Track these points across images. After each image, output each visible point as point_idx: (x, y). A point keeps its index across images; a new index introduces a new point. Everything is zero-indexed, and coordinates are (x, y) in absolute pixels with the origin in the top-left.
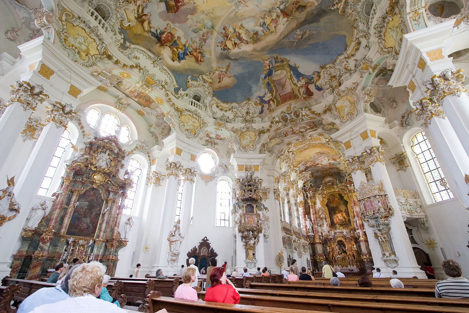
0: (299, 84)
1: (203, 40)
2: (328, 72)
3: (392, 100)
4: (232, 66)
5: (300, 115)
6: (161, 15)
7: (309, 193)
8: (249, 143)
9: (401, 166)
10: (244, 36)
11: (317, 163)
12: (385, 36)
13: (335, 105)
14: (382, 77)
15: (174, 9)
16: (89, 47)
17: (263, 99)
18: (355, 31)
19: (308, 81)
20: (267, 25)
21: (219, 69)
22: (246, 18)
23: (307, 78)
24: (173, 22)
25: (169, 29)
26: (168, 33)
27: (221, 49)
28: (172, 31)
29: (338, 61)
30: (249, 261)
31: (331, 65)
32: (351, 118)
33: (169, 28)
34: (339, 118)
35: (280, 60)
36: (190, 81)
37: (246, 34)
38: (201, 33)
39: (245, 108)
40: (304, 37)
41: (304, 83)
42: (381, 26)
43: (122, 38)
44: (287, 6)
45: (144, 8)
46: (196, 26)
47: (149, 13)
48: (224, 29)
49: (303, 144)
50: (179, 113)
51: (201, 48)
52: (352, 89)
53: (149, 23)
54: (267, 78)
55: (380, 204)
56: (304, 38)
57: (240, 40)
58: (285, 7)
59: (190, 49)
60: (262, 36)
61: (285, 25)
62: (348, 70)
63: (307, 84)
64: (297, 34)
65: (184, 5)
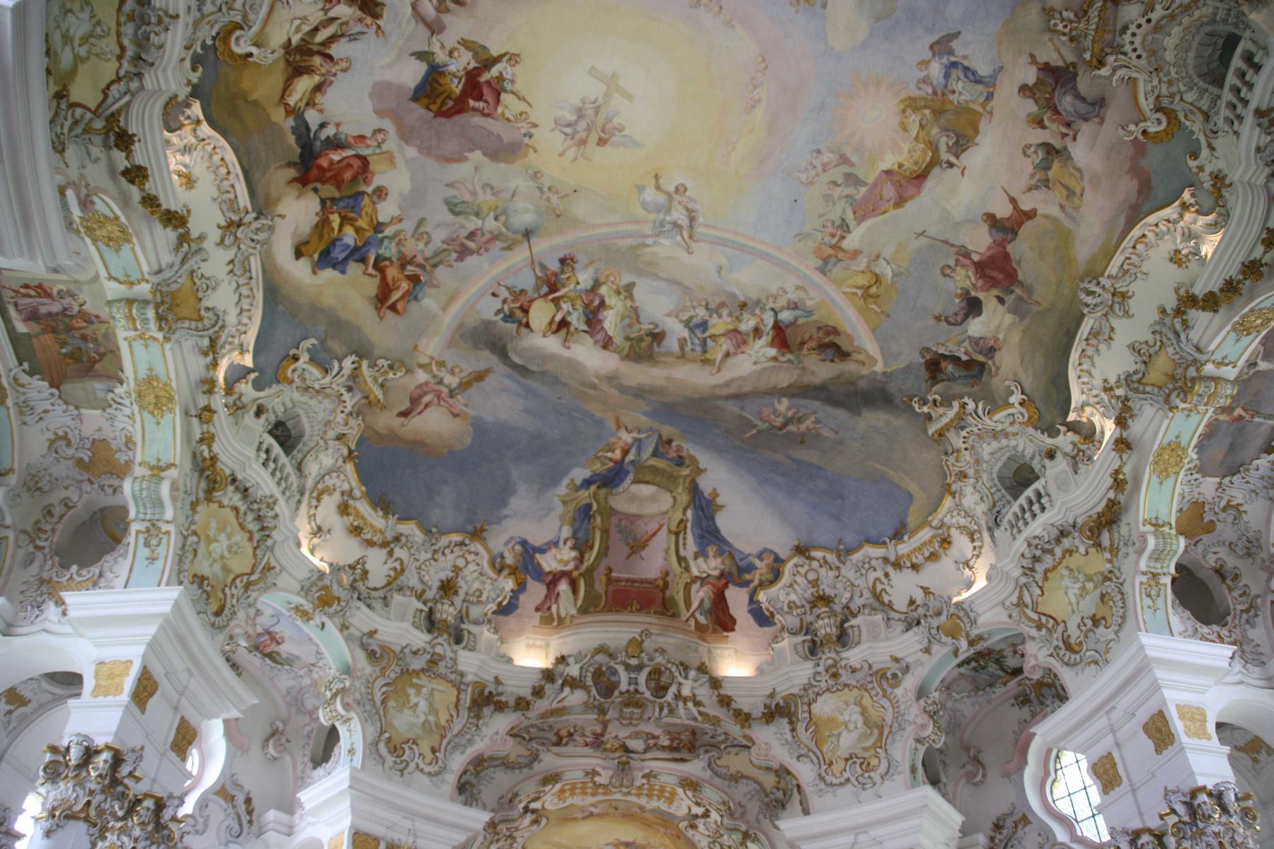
0: (698, 567)
1: (458, 248)
2: (811, 576)
3: (972, 752)
4: (490, 381)
5: (673, 690)
6: (381, 92)
8: (420, 731)
10: (610, 321)
12: (1046, 579)
13: (809, 705)
14: (973, 673)
15: (443, 104)
16: (82, 69)
17: (533, 558)
18: (948, 502)
19: (734, 570)
20: (707, 334)
21: (434, 369)
22: (660, 278)
23: (733, 558)
24: (406, 135)
25: (368, 146)
26: (357, 156)
27: (499, 311)
28: (375, 158)
29: (857, 557)
31: (831, 558)
32: (861, 779)
33: (375, 144)
34: (816, 761)
35: (672, 454)
36: (305, 357)
37: (623, 318)
38: (473, 223)
39: (449, 560)
40: (791, 428)
41: (716, 573)
42: (1047, 546)
43: (189, 83)
44: (800, 321)
45: (343, 35)
46: (474, 194)
47: (348, 60)
48: (563, 261)
49: (594, 795)
50: (203, 485)
51: (428, 268)
52: (884, 676)
53: (319, 88)
54: (593, 488)
56: (789, 433)
57: (589, 322)
58: (793, 324)
59: (389, 250)
60: (669, 354)
61: (758, 367)
62: (882, 603)
63: (726, 579)
64: (775, 411)
65: (488, 115)
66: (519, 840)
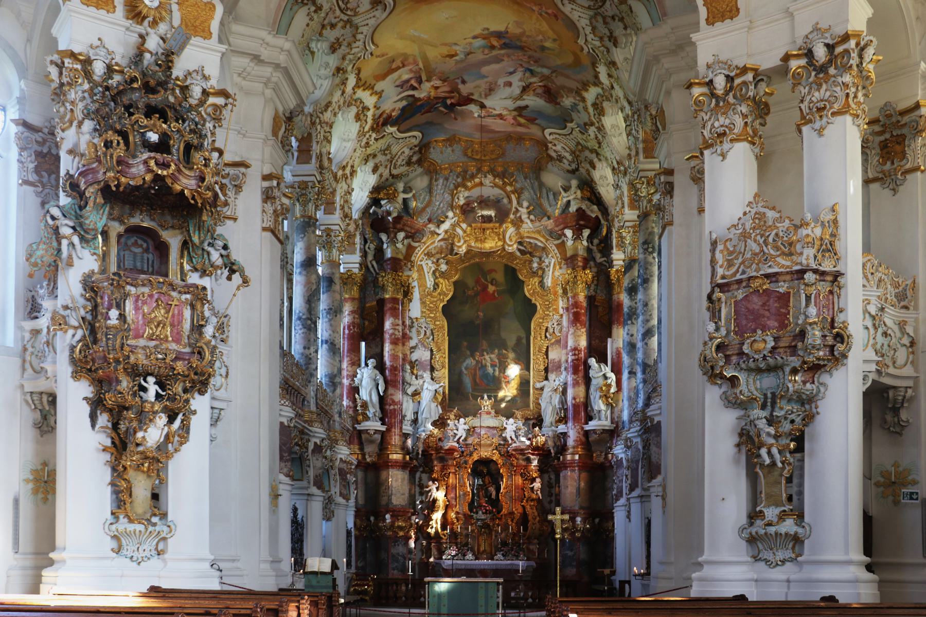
7: (393, 241)
9: (888, 166)
11: (464, 90)
30: (131, 527)
55: (813, 310)
66: (364, 29)
